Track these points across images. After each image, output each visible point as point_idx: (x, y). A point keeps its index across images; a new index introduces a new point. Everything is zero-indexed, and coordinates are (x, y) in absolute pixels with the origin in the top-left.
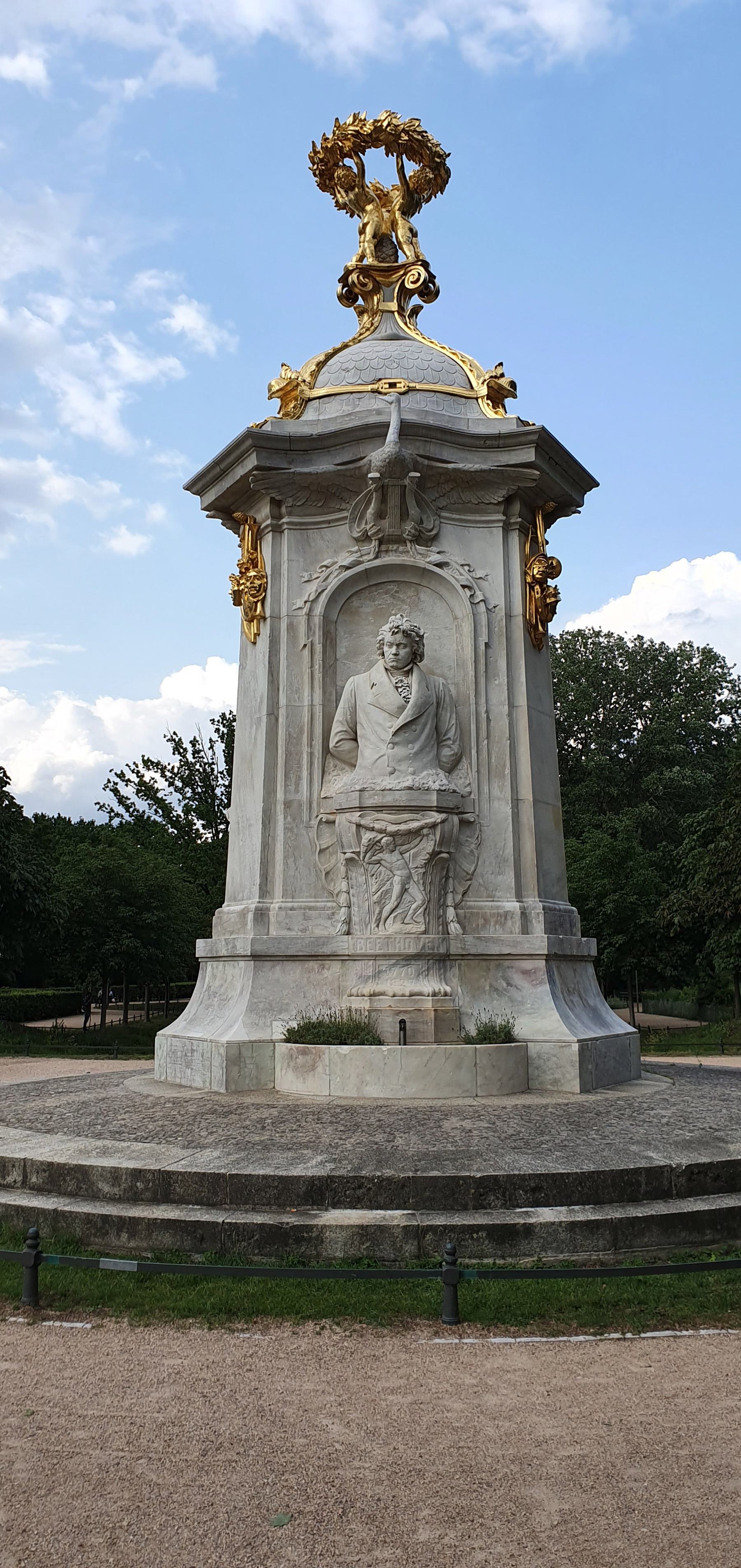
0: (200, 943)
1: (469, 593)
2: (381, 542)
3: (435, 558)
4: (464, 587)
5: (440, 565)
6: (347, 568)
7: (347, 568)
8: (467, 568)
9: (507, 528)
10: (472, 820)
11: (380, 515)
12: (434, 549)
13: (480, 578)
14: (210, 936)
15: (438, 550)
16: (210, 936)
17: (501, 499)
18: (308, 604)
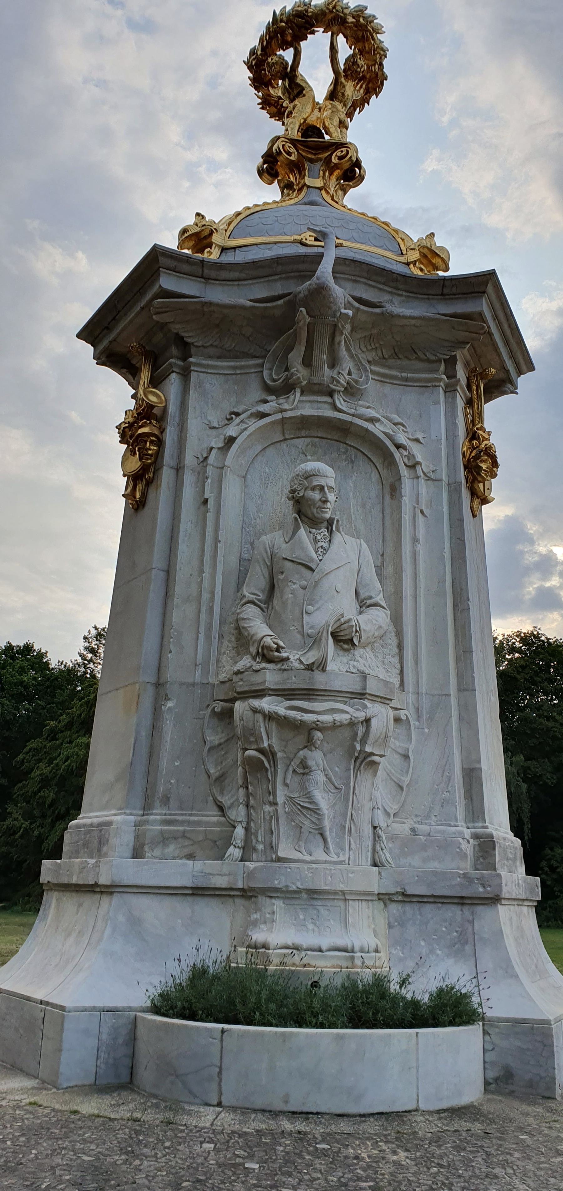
0: (46, 864)
1: (405, 453)
2: (302, 393)
4: (398, 446)
8: (401, 427)
10: (404, 718)
18: (214, 452)
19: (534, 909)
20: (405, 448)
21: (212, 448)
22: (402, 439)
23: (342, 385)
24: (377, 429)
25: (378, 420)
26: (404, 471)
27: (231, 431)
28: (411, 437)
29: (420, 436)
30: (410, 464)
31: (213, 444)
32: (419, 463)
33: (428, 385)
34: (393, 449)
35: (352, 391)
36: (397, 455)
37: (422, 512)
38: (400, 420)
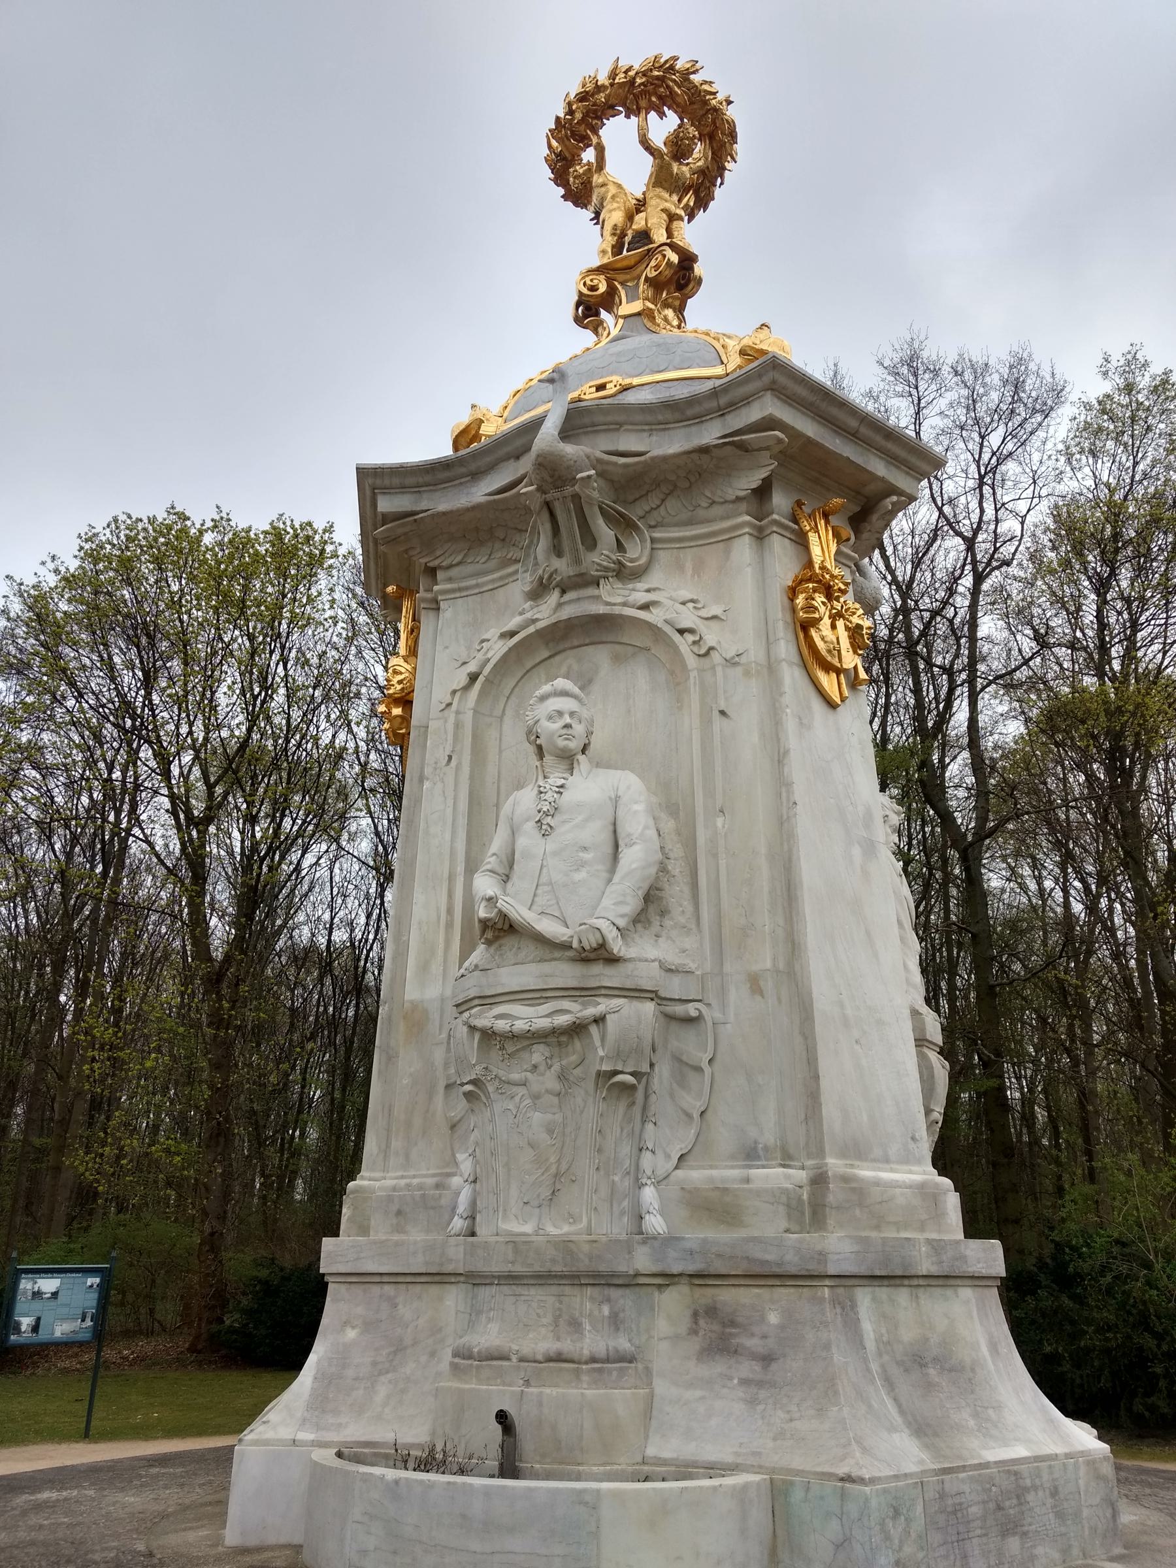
1: (690, 638)
3: (642, 597)
4: (681, 632)
5: (645, 607)
6: (512, 634)
7: (512, 634)
8: (691, 605)
9: (760, 536)
10: (694, 1013)
11: (558, 551)
12: (642, 586)
13: (714, 617)
14: (336, 1234)
15: (647, 586)
16: (338, 1236)
17: (742, 494)
18: (458, 695)
19: (995, 1291)
20: (691, 631)
21: (454, 692)
22: (687, 619)
23: (606, 569)
24: (654, 617)
25: (654, 603)
26: (691, 661)
27: (472, 667)
28: (705, 613)
29: (716, 610)
30: (702, 652)
31: (455, 687)
32: (711, 648)
33: (728, 538)
34: (676, 637)
35: (623, 573)
36: (684, 644)
37: (723, 713)
38: (689, 596)
